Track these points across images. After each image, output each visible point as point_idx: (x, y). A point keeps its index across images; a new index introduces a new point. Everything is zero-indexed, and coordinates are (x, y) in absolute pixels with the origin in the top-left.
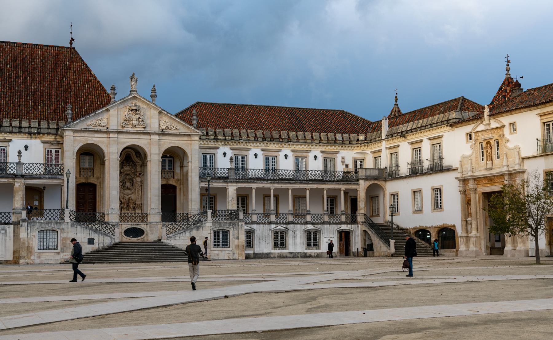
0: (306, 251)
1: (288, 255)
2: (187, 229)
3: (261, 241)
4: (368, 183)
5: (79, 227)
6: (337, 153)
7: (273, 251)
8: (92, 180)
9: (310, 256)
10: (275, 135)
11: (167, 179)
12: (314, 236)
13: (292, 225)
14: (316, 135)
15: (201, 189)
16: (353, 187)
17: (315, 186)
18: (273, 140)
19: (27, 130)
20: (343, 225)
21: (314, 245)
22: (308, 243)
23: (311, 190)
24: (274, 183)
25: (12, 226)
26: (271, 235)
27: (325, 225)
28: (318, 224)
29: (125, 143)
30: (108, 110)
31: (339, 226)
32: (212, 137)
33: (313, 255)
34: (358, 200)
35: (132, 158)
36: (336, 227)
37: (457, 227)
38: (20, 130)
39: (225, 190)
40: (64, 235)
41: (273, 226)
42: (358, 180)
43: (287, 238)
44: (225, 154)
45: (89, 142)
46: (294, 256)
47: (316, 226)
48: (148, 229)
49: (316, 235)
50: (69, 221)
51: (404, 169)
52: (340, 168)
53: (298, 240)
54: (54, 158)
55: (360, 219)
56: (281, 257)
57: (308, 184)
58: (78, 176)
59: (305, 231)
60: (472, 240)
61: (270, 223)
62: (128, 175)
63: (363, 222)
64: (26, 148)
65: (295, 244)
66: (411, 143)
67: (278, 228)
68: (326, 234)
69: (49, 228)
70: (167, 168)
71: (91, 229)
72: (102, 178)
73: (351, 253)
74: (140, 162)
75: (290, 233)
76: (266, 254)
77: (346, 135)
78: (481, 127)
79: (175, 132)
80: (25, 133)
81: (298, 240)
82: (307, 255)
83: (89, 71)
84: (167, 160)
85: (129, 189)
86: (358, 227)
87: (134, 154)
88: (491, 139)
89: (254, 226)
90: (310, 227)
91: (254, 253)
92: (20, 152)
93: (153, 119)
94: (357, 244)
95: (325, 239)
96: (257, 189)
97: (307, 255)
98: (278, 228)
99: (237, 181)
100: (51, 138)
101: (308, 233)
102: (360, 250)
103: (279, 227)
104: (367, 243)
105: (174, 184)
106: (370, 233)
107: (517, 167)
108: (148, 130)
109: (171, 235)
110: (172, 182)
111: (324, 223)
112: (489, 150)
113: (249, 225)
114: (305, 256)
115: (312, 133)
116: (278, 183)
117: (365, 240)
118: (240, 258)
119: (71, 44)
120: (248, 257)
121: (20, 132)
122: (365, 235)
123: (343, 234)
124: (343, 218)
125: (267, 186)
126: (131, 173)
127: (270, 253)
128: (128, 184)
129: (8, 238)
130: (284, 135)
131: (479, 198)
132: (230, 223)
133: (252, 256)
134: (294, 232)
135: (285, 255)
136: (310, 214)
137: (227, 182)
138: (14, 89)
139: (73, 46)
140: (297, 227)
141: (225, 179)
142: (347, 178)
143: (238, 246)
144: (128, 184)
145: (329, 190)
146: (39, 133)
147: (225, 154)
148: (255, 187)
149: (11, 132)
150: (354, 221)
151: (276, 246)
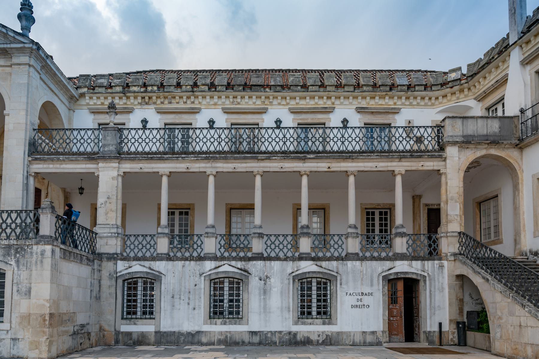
0: (295, 328)
1: (246, 338)
3: (177, 300)
7: (206, 328)
9: (307, 342)
12: (319, 289)
13: (260, 264)
21: (319, 313)
22: (302, 307)
26: (204, 286)
27: (349, 263)
28: (330, 259)
31: (388, 264)
33: (314, 338)
36: (380, 268)
41: (209, 265)
43: (245, 296)
47: (324, 264)
49: (325, 289)
56: (229, 343)
59: (294, 278)
63: (455, 255)
65: (266, 310)
67: (221, 269)
68: (351, 284)
73: (422, 336)
75: (254, 283)
82: (299, 338)
90: (307, 267)
94: (438, 310)
95: (348, 298)
97: (299, 338)
98: (221, 269)
99: (120, 155)
101: (303, 282)
102: (446, 328)
103: (226, 268)
104: (466, 309)
106: (477, 280)
113: (147, 264)
114: (294, 342)
117: (461, 301)
122: (462, 287)
123: (400, 286)
125: (197, 166)
127: (198, 332)
134: (265, 279)
135: (237, 338)
136: (308, 234)
140: (272, 268)
148: (167, 171)
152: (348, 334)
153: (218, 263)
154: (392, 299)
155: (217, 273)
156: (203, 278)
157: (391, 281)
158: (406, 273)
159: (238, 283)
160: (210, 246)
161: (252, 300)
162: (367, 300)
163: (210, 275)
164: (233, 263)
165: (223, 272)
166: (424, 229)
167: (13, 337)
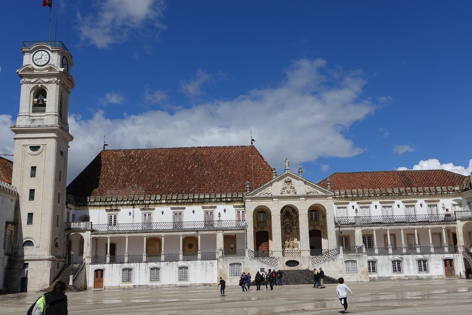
0: (418, 275)
2: (326, 261)
3: (383, 268)
4: (464, 223)
5: (254, 261)
6: (438, 201)
7: (392, 275)
8: (266, 229)
9: (422, 279)
10: (390, 191)
11: (314, 226)
13: (406, 256)
14: (420, 189)
15: (336, 232)
16: (452, 226)
17: (421, 227)
18: (388, 194)
19: (225, 200)
20: (446, 255)
23: (418, 229)
24: (390, 226)
25: (216, 261)
26: (391, 264)
29: (283, 203)
30: (271, 184)
31: (443, 255)
32: (344, 196)
33: (424, 277)
34: (457, 235)
35: (289, 215)
36: (441, 256)
38: (220, 201)
39: (354, 231)
40: (245, 266)
41: (391, 257)
42: (455, 220)
44: (353, 207)
45: (261, 205)
46: (410, 279)
47: (424, 255)
48: (302, 261)
50: (248, 257)
52: (442, 213)
53: (411, 267)
54: (241, 216)
55: (461, 250)
57: (415, 225)
58: (257, 227)
61: (389, 255)
62: (288, 225)
64: (225, 211)
65: (409, 269)
68: (433, 261)
69: (236, 262)
70: (314, 218)
71: (262, 262)
72: (270, 227)
74: (296, 216)
76: (387, 277)
77: (444, 188)
79: (316, 194)
80: (224, 202)
81: (411, 267)
83: (263, 159)
84: (313, 213)
85: (289, 234)
86: (459, 255)
87: (291, 210)
89: (377, 257)
90: (420, 257)
91: (378, 277)
92: (219, 214)
93: (300, 187)
96: (377, 231)
97: (420, 277)
100: (239, 204)
101: (419, 261)
105: (319, 229)
108: (298, 194)
109: (315, 265)
110: (318, 228)
111: (430, 253)
113: (373, 257)
114: (418, 279)
115: (417, 187)
116: (392, 226)
118: (366, 280)
119: (252, 143)
120: (372, 280)
121: (221, 201)
124: (446, 249)
125: (384, 228)
126: (290, 224)
128: (288, 231)
129: (214, 269)
130: (396, 190)
132: (356, 255)
133: (377, 279)
134: (408, 260)
137: (355, 227)
138: (219, 174)
139: (253, 145)
141: (353, 224)
142: (448, 219)
143: (363, 272)
144: (288, 231)
145: (432, 229)
146: (231, 201)
147: (353, 207)
149: (216, 202)
150: (455, 251)
151: (395, 270)
152: (434, 276)
154: (446, 266)
157: (445, 261)
159: (399, 262)
161: (404, 266)
162: (438, 266)
166: (452, 243)
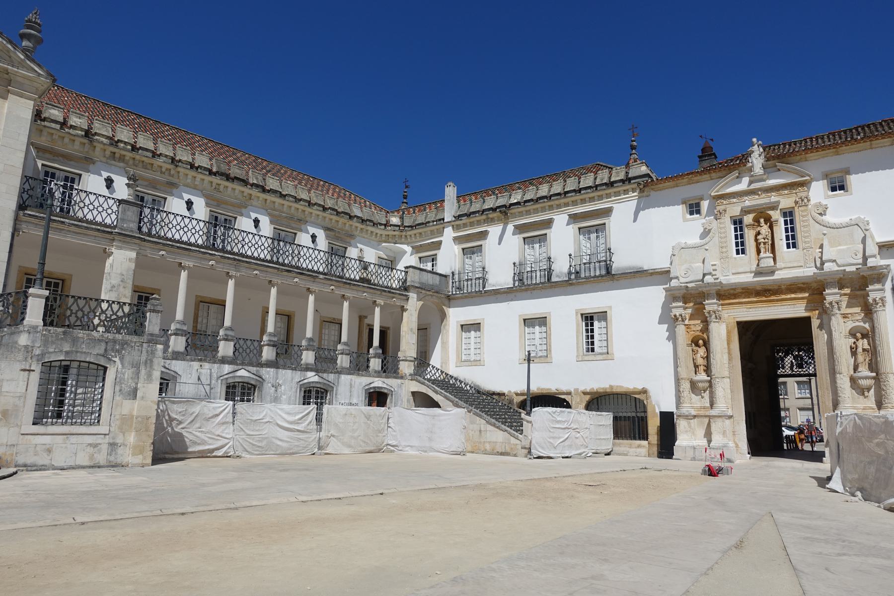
37: (652, 393)
41: (227, 368)
47: (325, 375)
51: (501, 276)
60: (719, 426)
66: (519, 229)
78: (743, 185)
88: (774, 207)
89: (177, 366)
90: (312, 377)
103: (243, 373)
107: (871, 262)
112: (765, 229)
118: (138, 459)
131: (729, 333)
134: (276, 387)
153: (236, 367)
155: (234, 377)
156: (219, 381)
158: (381, 388)
160: (308, 357)
163: (227, 379)
164: (250, 368)
165: (240, 377)
167: (111, 441)
